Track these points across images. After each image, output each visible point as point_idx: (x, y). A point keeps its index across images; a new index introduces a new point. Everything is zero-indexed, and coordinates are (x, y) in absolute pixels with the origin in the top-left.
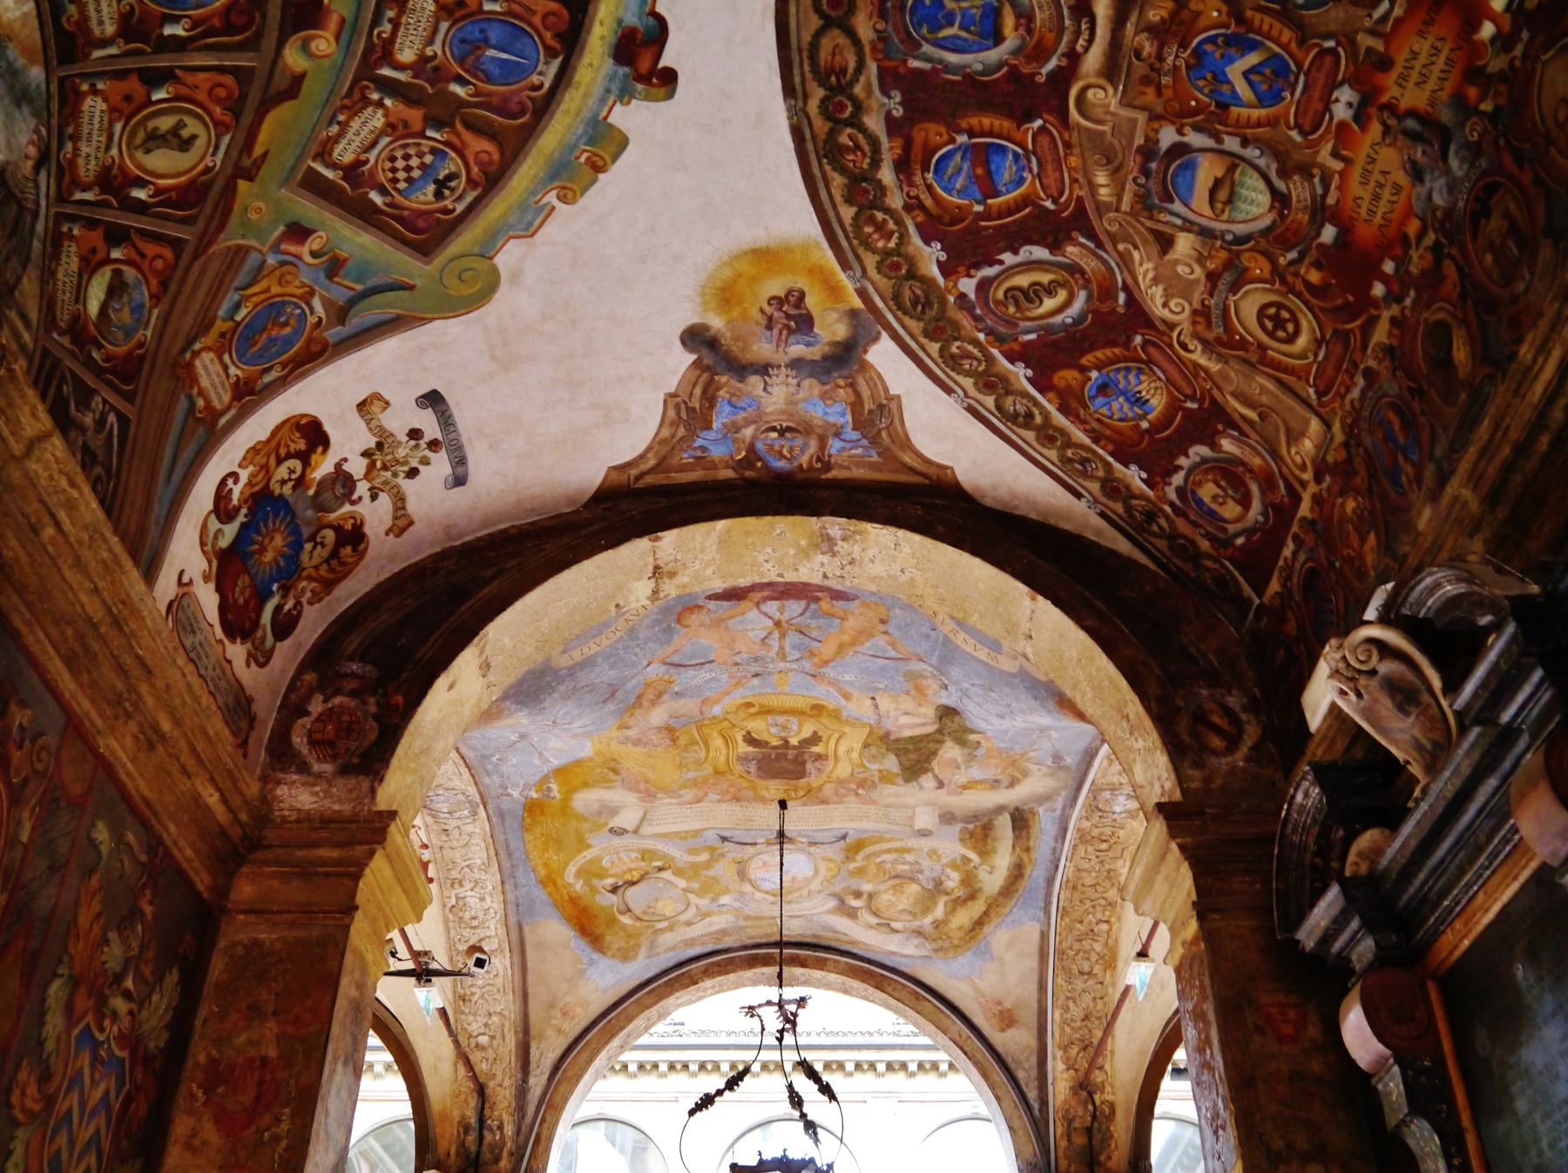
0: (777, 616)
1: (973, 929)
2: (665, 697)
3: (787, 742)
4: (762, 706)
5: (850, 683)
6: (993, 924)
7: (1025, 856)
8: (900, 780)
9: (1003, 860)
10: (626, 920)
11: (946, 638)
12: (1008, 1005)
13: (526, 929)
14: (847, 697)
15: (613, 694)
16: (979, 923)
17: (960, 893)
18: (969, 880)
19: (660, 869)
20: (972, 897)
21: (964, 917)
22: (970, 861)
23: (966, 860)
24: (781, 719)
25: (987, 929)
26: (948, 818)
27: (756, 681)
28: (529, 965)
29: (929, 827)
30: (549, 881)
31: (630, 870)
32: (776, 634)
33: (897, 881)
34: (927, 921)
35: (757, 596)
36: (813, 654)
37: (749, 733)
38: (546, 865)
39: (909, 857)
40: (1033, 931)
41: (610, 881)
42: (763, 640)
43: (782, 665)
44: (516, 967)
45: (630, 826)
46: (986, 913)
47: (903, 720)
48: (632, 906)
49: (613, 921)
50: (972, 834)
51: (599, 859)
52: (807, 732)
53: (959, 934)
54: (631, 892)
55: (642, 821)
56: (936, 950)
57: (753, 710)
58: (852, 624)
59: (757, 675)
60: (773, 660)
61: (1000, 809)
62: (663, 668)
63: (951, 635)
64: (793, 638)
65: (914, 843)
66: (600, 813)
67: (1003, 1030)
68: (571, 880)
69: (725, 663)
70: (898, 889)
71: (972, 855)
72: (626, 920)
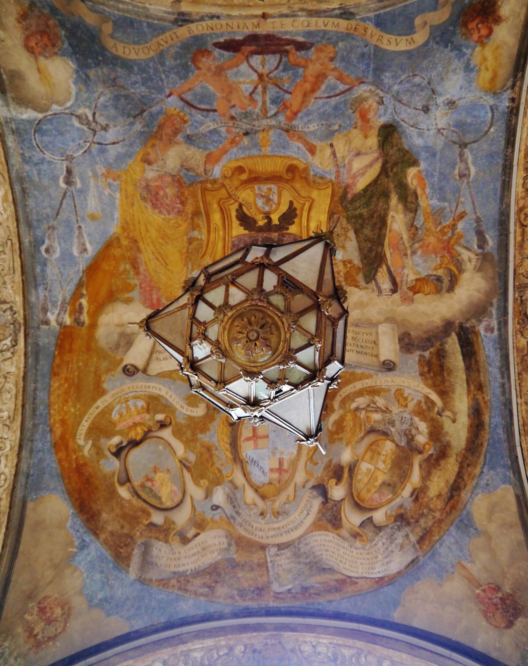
0: (260, 69)
1: (451, 497)
2: (180, 138)
3: (270, 220)
4: (251, 172)
5: (313, 133)
6: (469, 487)
7: (479, 397)
8: (360, 278)
9: (462, 403)
10: (124, 492)
11: (376, 47)
12: (507, 589)
13: (30, 505)
14: (312, 150)
15: (143, 111)
16: (456, 488)
17: (431, 451)
18: (436, 433)
19: (163, 425)
20: (443, 453)
21: (439, 484)
22: (433, 403)
23: (431, 403)
24: (265, 188)
25: (465, 495)
26: (407, 343)
27: (246, 141)
28: (21, 548)
29: (392, 358)
30: (63, 444)
31: (135, 425)
32: (260, 89)
33: (372, 438)
34: (406, 492)
35: (247, 49)
36: (286, 107)
37: (240, 205)
38: (63, 422)
39: (380, 402)
40: (507, 494)
41: (116, 440)
42: (251, 94)
43: (265, 122)
44: (7, 549)
45: (140, 363)
46: (459, 475)
47: (357, 165)
48: (131, 474)
49: (113, 494)
50: (429, 363)
51: (107, 411)
52: (284, 208)
53: (440, 504)
54: (135, 456)
55: (152, 353)
56: (421, 540)
57: (244, 177)
58: (313, 69)
59: (246, 134)
60: (258, 116)
61: (448, 326)
62: (181, 104)
63: (379, 44)
64: (272, 91)
65: (383, 380)
66: (117, 346)
67: (510, 624)
68: (81, 442)
69: (224, 115)
70: (373, 450)
71: (434, 397)
72: (124, 492)
